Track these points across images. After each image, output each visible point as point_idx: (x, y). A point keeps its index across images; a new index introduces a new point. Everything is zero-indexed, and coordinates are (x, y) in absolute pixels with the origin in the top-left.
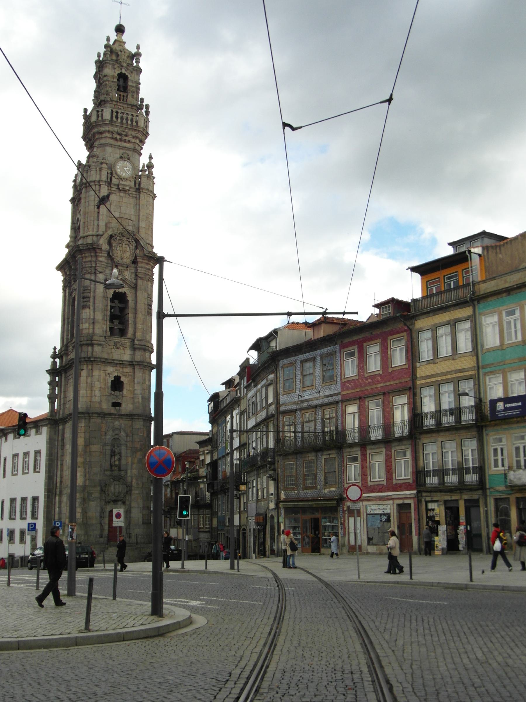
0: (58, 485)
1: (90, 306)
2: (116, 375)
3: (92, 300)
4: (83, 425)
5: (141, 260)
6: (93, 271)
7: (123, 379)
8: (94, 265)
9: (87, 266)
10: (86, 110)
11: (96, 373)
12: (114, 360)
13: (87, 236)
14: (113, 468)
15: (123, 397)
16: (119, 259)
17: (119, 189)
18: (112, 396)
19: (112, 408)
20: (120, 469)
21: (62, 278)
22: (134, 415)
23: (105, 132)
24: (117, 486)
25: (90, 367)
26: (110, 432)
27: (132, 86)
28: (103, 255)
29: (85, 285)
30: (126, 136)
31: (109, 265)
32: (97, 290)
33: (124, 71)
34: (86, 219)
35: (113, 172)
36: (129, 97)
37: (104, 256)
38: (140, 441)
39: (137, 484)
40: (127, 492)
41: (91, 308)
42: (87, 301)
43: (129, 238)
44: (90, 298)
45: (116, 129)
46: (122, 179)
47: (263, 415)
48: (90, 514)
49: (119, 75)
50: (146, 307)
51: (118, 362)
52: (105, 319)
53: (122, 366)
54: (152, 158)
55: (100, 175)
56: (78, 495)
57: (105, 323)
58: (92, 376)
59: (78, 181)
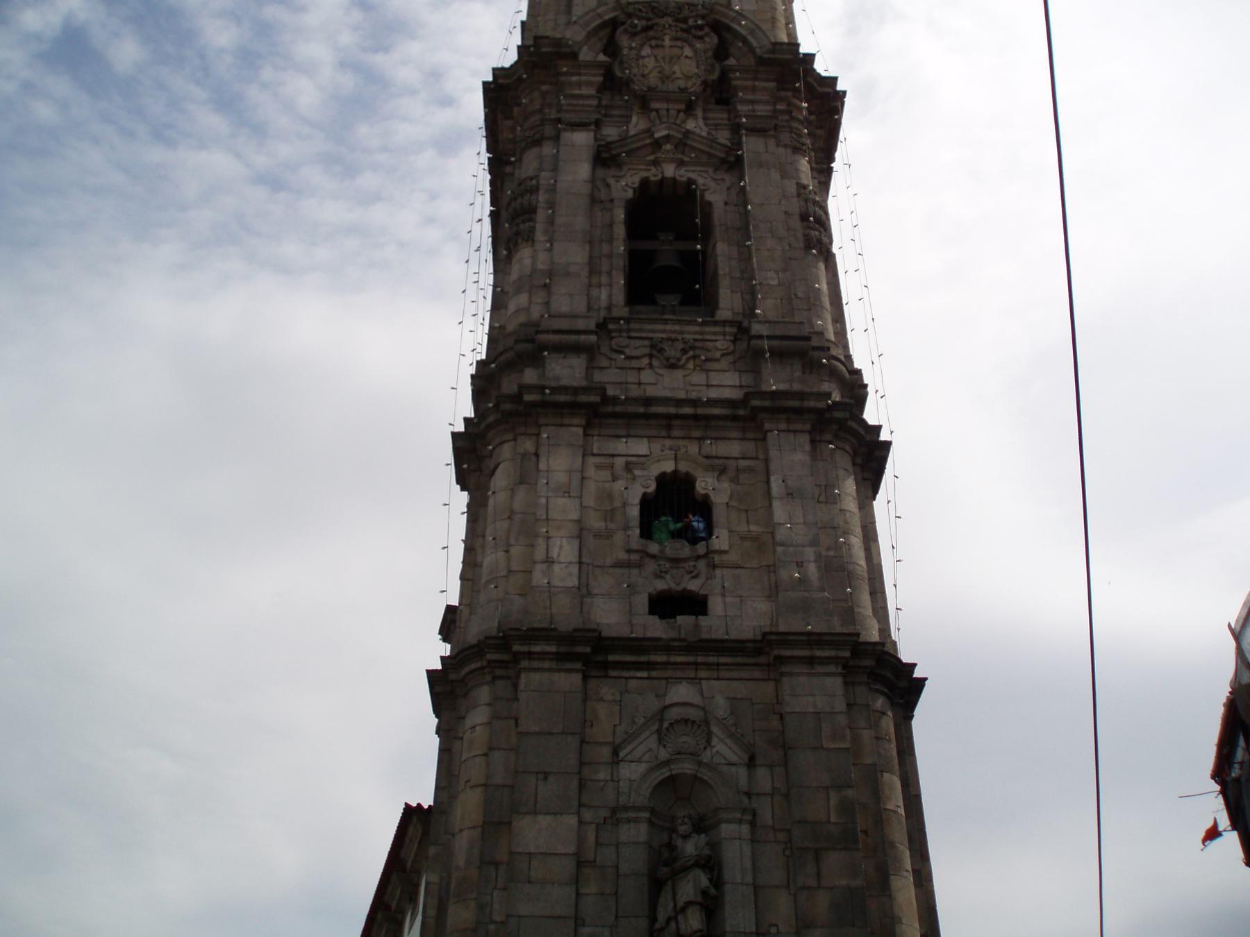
1: (532, 230)
2: (669, 467)
3: (541, 215)
5: (750, 83)
6: (548, 130)
7: (705, 484)
11: (559, 462)
12: (648, 401)
15: (714, 567)
16: (653, 80)
18: (651, 566)
19: (655, 619)
22: (786, 639)
26: (647, 745)
31: (616, 112)
37: (589, 84)
41: (540, 236)
44: (531, 211)
50: (796, 223)
51: (672, 410)
52: (605, 268)
53: (696, 434)
57: (604, 280)
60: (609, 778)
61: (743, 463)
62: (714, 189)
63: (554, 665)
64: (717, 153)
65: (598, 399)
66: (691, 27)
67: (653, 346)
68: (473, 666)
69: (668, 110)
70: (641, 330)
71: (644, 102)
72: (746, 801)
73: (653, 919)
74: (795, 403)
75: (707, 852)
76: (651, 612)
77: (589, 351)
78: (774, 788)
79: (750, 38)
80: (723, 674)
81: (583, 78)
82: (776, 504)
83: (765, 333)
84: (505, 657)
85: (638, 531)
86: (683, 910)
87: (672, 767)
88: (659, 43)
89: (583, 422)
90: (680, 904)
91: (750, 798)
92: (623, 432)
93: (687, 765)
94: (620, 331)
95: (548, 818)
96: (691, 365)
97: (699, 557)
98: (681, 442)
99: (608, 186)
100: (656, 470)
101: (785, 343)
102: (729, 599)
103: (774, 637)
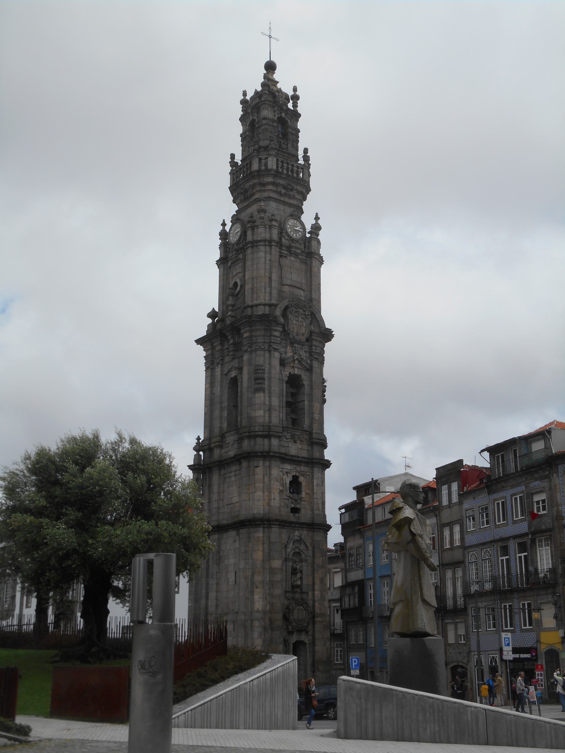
0: (212, 609)
3: (266, 382)
4: (261, 535)
5: (316, 338)
6: (267, 346)
7: (301, 479)
8: (267, 341)
9: (259, 341)
10: (233, 156)
11: (275, 472)
13: (257, 305)
17: (290, 252)
20: (302, 592)
21: (204, 354)
22: (317, 525)
23: (268, 184)
25: (267, 464)
27: (293, 134)
28: (278, 328)
29: (257, 363)
30: (292, 190)
31: (283, 342)
32: (273, 371)
33: (283, 115)
34: (255, 285)
36: (289, 145)
37: (279, 331)
41: (267, 392)
42: (261, 384)
43: (305, 311)
44: (264, 379)
45: (281, 182)
46: (292, 240)
47: (523, 528)
49: (278, 118)
52: (281, 406)
54: (319, 218)
55: (271, 234)
56: (256, 623)
57: (281, 411)
58: (270, 474)
59: (233, 239)
62: (305, 377)
67: (292, 436)
71: (292, 344)
74: (321, 462)
77: (279, 437)
81: (278, 328)
86: (297, 580)
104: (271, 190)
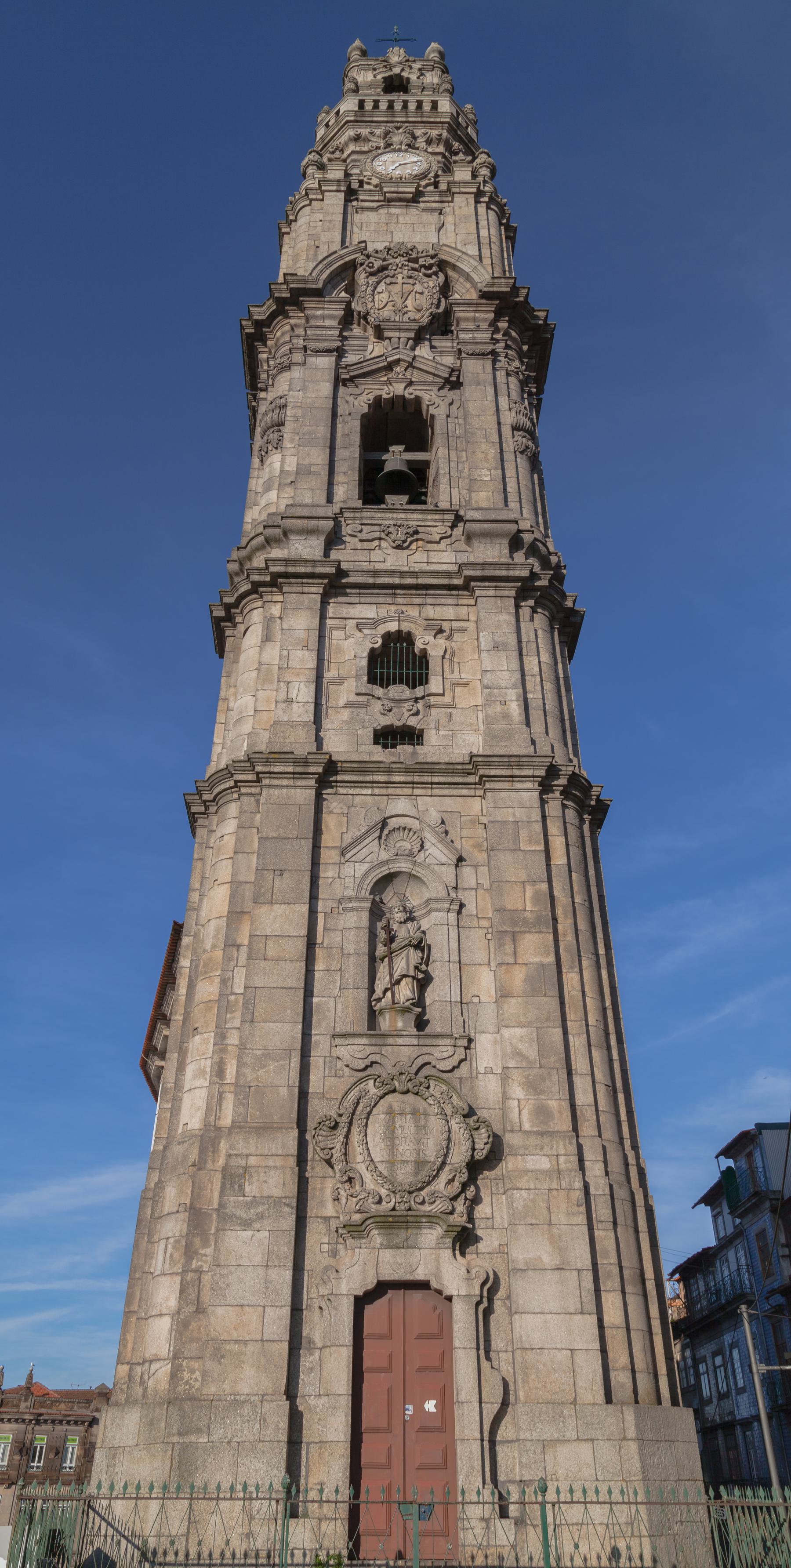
2: (393, 627)
4: (230, 827)
5: (471, 315)
6: (298, 357)
12: (376, 573)
14: (385, 1023)
15: (430, 707)
16: (386, 313)
18: (377, 706)
22: (488, 760)
24: (406, 1126)
35: (365, 174)
37: (331, 317)
38: (534, 882)
39: (542, 1112)
40: (475, 1168)
41: (287, 443)
43: (416, 260)
48: (221, 1319)
49: (384, 78)
50: (507, 431)
51: (397, 581)
53: (417, 601)
60: (336, 876)
61: (456, 624)
63: (291, 782)
64: (440, 374)
65: (333, 570)
66: (421, 266)
68: (223, 787)
69: (399, 338)
70: (372, 518)
72: (453, 895)
73: (372, 991)
74: (503, 573)
75: (418, 934)
76: (376, 742)
78: (477, 884)
79: (472, 274)
80: (436, 792)
81: (326, 312)
82: (484, 655)
83: (480, 518)
84: (251, 777)
85: (365, 678)
86: (398, 982)
87: (391, 866)
88: (393, 280)
89: (321, 590)
90: (396, 976)
91: (456, 892)
92: (357, 600)
93: (403, 865)
94: (354, 519)
95: (283, 906)
96: (414, 546)
97: (416, 700)
98: (404, 608)
99: (347, 402)
100: (382, 629)
101: (495, 526)
102: (442, 733)
103: (480, 759)
104: (353, 152)
